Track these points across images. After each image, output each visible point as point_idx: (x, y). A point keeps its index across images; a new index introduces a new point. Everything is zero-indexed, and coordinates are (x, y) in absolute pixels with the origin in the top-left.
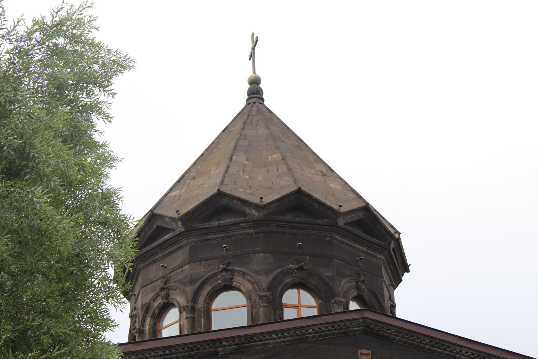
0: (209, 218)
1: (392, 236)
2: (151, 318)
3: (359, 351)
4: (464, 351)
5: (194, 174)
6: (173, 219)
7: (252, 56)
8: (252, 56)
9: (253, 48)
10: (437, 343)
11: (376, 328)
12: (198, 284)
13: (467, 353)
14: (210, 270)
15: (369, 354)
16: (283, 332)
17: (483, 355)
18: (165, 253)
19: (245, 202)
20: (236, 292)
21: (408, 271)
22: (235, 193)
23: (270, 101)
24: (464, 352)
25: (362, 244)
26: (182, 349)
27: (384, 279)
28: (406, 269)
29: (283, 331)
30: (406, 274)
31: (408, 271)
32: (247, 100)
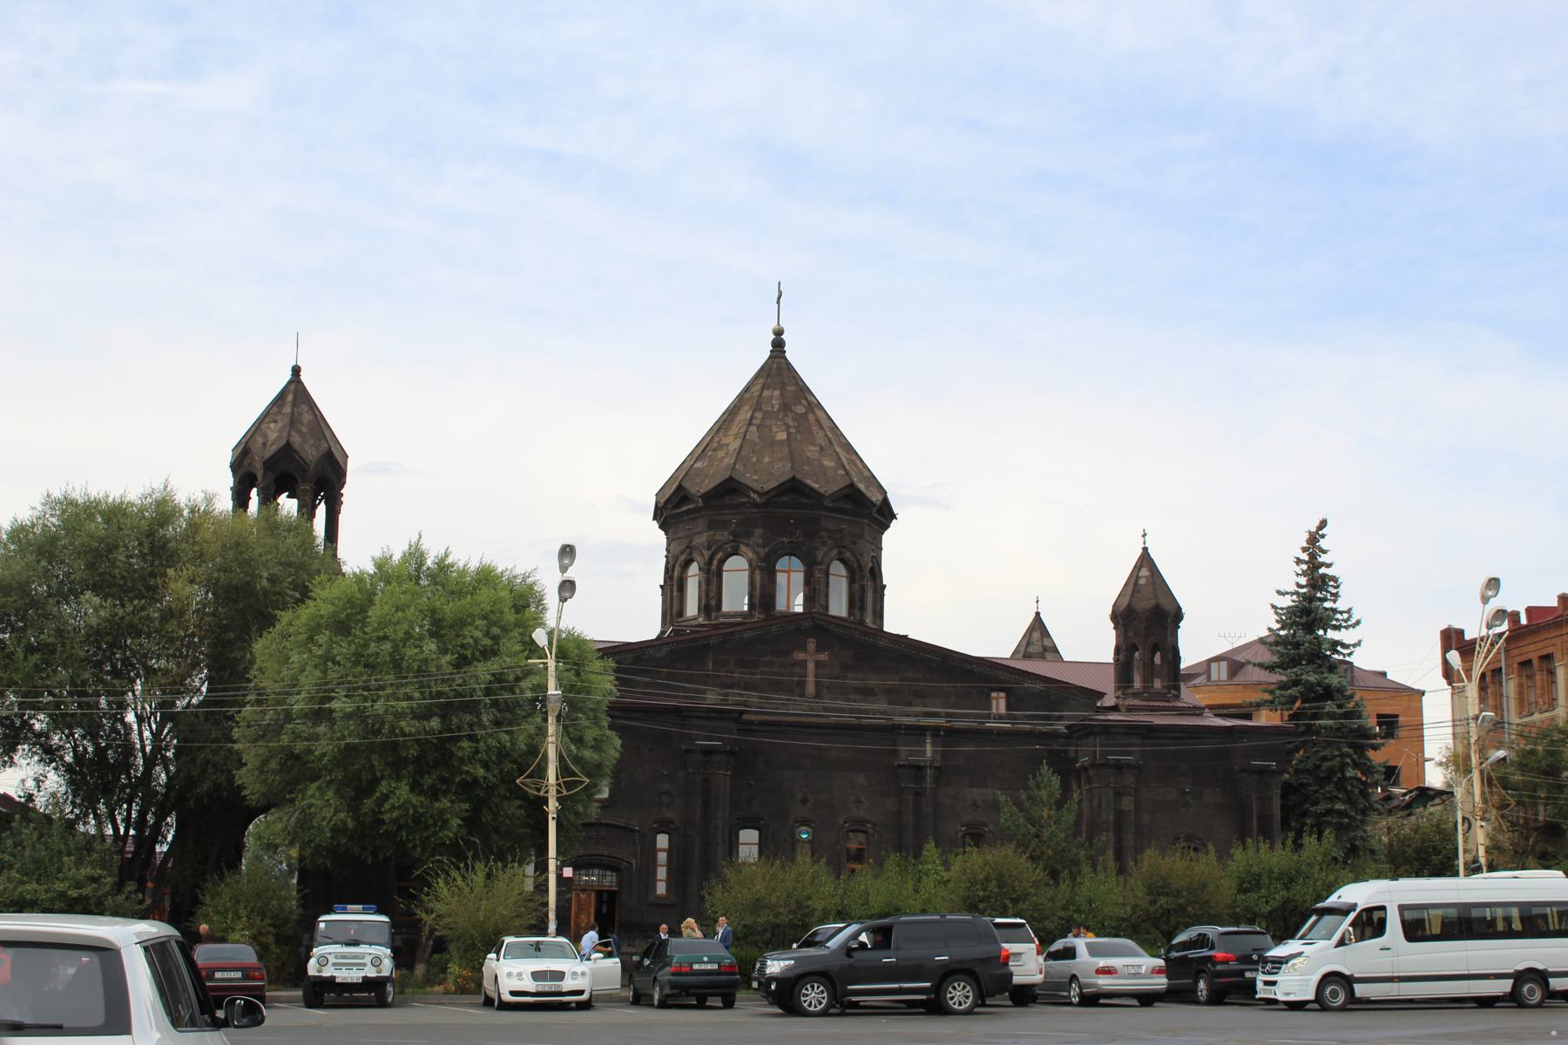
7: (778, 302)
8: (778, 302)
19: (750, 488)
23: (791, 354)
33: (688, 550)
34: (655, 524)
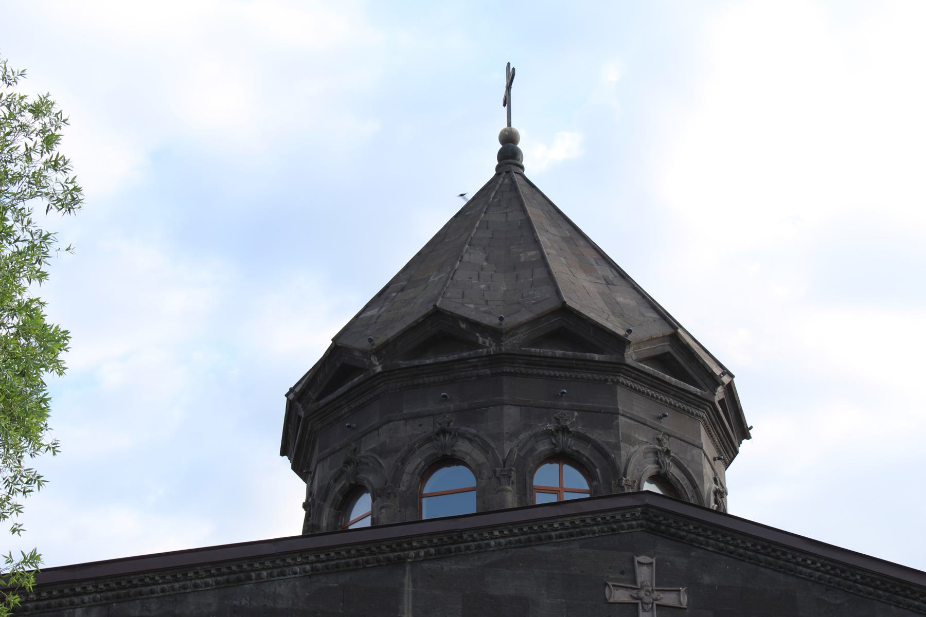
0: (422, 349)
1: (714, 381)
2: (331, 507)
3: (637, 559)
4: (809, 560)
5: (404, 283)
6: (365, 353)
7: (507, 102)
8: (507, 102)
9: (509, 88)
15: (651, 563)
16: (510, 527)
18: (353, 406)
19: (475, 325)
20: (462, 468)
21: (748, 437)
22: (461, 312)
25: (667, 393)
26: (347, 552)
27: (705, 448)
28: (745, 433)
30: (745, 441)
31: (748, 437)
32: (498, 168)
33: (349, 469)
34: (286, 462)
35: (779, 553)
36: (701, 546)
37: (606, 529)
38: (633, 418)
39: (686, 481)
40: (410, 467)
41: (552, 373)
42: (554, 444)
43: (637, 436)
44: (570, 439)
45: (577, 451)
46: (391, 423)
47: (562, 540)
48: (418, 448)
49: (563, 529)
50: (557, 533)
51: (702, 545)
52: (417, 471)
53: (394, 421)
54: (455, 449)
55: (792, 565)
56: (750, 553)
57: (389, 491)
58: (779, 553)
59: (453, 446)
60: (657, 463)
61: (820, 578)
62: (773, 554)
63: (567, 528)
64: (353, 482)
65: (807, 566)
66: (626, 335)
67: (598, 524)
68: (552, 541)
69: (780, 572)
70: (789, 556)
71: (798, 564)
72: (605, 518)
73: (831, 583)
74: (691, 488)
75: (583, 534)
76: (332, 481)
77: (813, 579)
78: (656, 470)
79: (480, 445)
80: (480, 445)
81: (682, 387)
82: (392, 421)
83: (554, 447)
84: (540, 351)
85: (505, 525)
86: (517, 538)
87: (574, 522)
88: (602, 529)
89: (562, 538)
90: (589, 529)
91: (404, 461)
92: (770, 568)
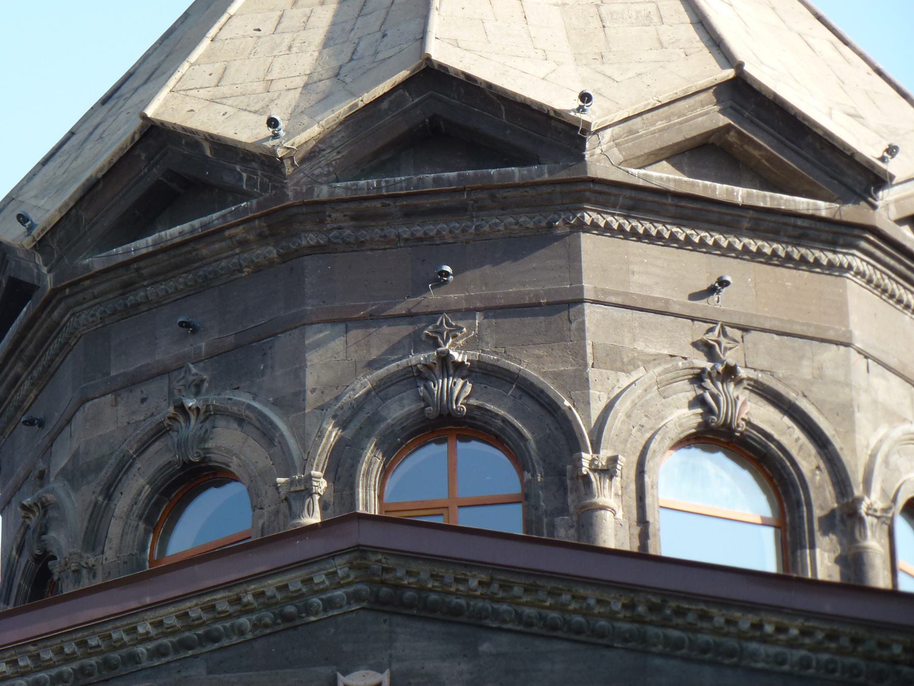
4: (770, 623)
10: (652, 608)
11: (412, 580)
12: (105, 474)
13: (780, 629)
14: (142, 418)
17: (847, 629)
24: (769, 629)
29: (34, 644)
35: (691, 618)
36: (505, 626)
37: (268, 620)
38: (627, 303)
39: (797, 433)
40: (122, 504)
41: (419, 231)
42: (423, 399)
43: (640, 346)
44: (460, 382)
45: (478, 408)
46: (88, 405)
47: (164, 660)
48: (138, 456)
49: (165, 635)
50: (151, 646)
51: (504, 621)
52: (137, 510)
53: (92, 399)
54: (210, 444)
55: (732, 643)
56: (626, 626)
57: (73, 567)
58: (691, 618)
59: (203, 439)
60: (699, 401)
61: (805, 664)
62: (680, 621)
63: (174, 632)
64: (37, 552)
65: (765, 639)
66: (581, 109)
67: (247, 610)
68: (140, 667)
69: (702, 662)
70: (719, 620)
71: (742, 636)
72: (263, 593)
73: (833, 671)
74: (811, 448)
75: (216, 640)
76: (14, 553)
77: (786, 668)
78: (700, 420)
79: (258, 429)
80: (258, 429)
81: (768, 205)
82: (88, 401)
83: (422, 405)
84: (379, 183)
85: (19, 645)
86: (54, 672)
87: (186, 614)
88: (260, 620)
89: (164, 655)
90: (228, 624)
91: (109, 492)
92: (675, 657)
